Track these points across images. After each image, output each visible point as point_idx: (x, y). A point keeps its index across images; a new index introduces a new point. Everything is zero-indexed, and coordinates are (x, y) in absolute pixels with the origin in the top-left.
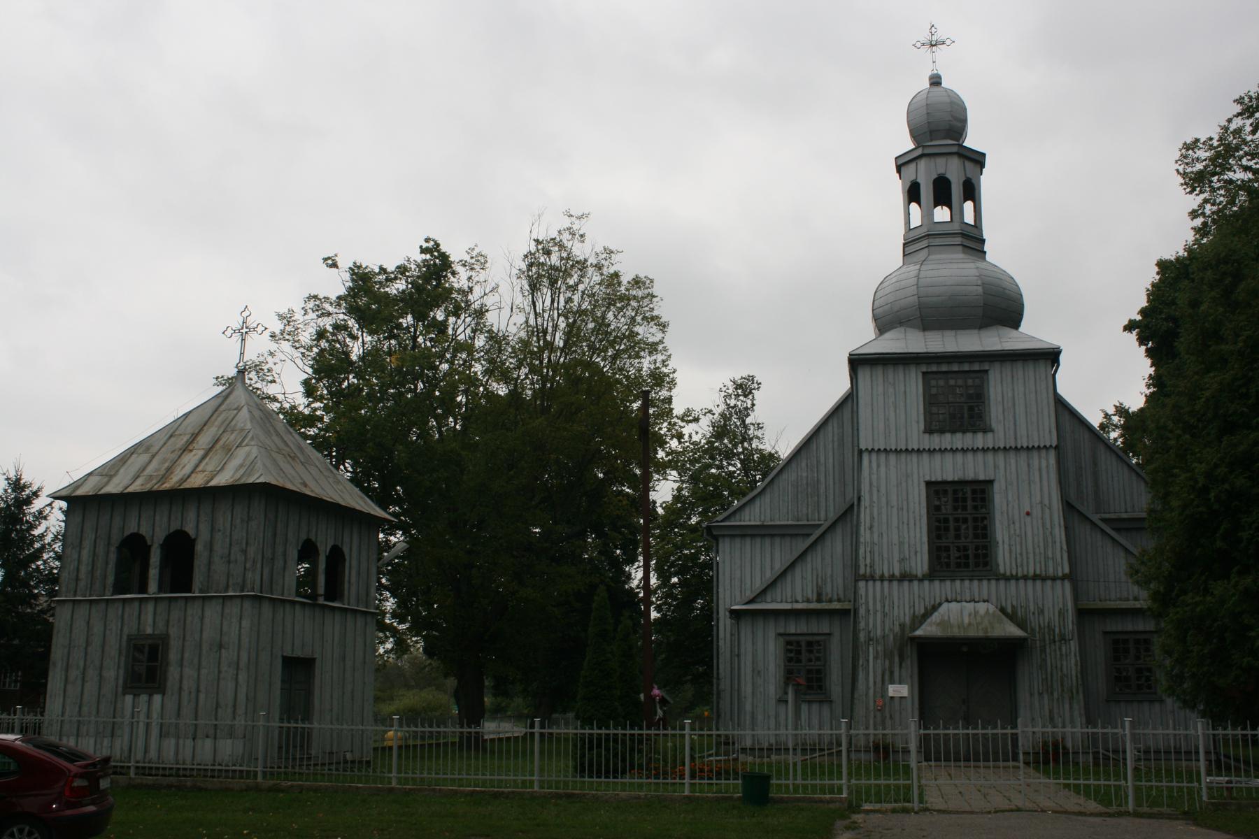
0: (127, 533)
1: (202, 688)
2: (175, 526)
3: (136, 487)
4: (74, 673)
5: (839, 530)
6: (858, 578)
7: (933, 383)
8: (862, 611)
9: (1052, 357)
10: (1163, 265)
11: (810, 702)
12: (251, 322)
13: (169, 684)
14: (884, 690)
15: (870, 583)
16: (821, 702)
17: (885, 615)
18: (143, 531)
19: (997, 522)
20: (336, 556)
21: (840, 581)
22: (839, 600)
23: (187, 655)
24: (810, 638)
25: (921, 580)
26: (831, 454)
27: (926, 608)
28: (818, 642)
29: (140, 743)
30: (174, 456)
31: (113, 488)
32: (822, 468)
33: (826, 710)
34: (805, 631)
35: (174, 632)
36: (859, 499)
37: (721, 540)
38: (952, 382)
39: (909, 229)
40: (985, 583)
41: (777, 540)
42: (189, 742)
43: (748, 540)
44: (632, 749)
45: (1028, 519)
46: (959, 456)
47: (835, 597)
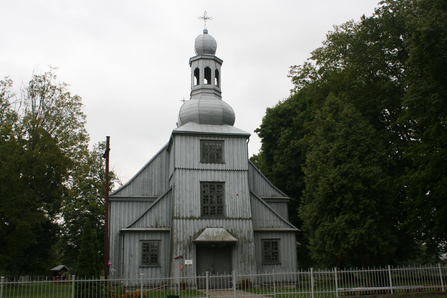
5: (165, 199)
8: (175, 231)
10: (269, 110)
11: (152, 267)
15: (178, 220)
17: (184, 233)
19: (226, 198)
21: (165, 219)
22: (164, 227)
25: (198, 219)
26: (157, 170)
27: (199, 230)
32: (153, 176)
33: (158, 270)
34: (151, 239)
37: (112, 203)
38: (211, 144)
41: (135, 203)
43: (123, 203)
45: (237, 197)
46: (213, 172)
47: (163, 226)
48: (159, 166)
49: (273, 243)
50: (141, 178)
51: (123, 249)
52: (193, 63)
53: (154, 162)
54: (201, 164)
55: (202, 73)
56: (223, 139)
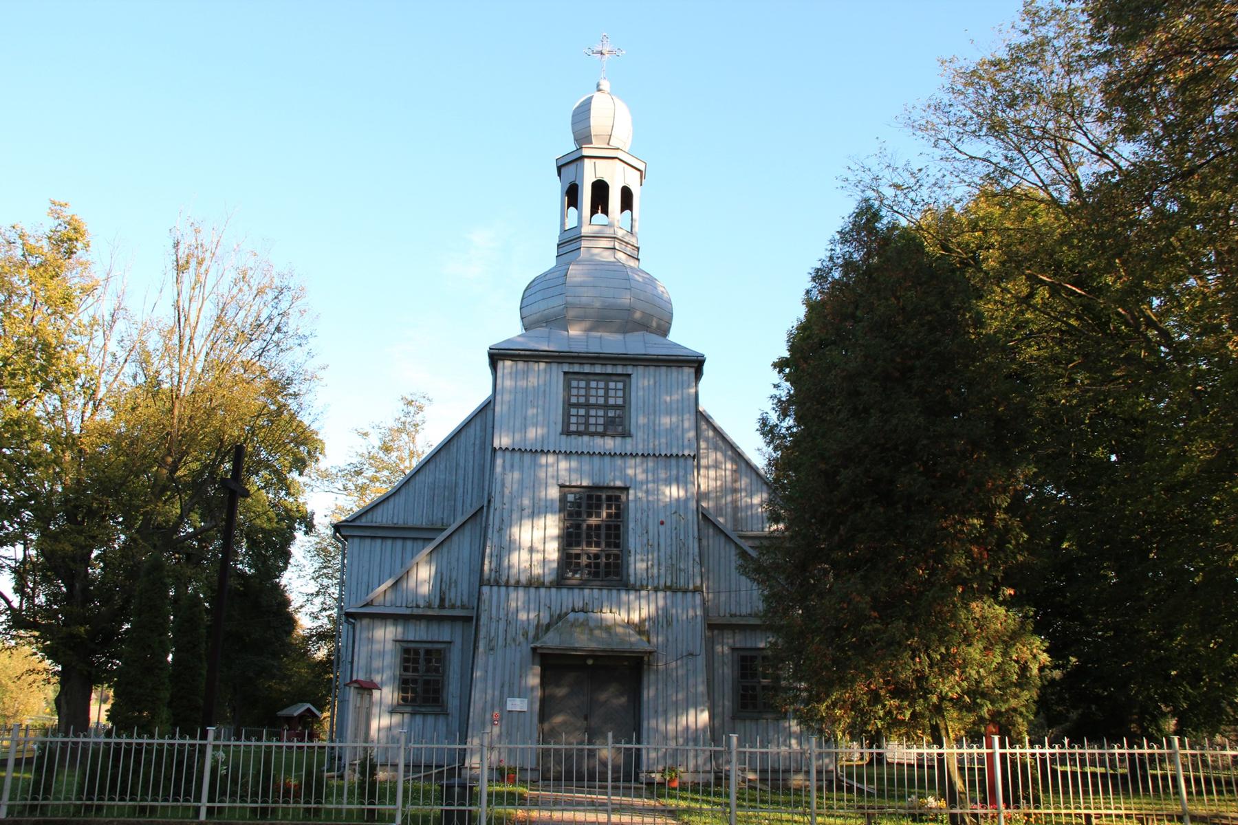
6: (482, 583)
7: (574, 383)
9: (696, 364)
11: (425, 714)
14: (503, 704)
15: (495, 589)
16: (437, 714)
17: (508, 623)
21: (465, 586)
22: (463, 607)
26: (471, 457)
27: (551, 616)
28: (439, 651)
32: (461, 472)
33: (441, 720)
34: (425, 638)
36: (489, 501)
39: (563, 231)
40: (614, 592)
43: (379, 542)
45: (662, 528)
46: (596, 459)
47: (459, 603)
48: (477, 448)
50: (426, 478)
51: (352, 662)
52: (563, 170)
53: (464, 433)
54: (564, 437)
56: (629, 370)
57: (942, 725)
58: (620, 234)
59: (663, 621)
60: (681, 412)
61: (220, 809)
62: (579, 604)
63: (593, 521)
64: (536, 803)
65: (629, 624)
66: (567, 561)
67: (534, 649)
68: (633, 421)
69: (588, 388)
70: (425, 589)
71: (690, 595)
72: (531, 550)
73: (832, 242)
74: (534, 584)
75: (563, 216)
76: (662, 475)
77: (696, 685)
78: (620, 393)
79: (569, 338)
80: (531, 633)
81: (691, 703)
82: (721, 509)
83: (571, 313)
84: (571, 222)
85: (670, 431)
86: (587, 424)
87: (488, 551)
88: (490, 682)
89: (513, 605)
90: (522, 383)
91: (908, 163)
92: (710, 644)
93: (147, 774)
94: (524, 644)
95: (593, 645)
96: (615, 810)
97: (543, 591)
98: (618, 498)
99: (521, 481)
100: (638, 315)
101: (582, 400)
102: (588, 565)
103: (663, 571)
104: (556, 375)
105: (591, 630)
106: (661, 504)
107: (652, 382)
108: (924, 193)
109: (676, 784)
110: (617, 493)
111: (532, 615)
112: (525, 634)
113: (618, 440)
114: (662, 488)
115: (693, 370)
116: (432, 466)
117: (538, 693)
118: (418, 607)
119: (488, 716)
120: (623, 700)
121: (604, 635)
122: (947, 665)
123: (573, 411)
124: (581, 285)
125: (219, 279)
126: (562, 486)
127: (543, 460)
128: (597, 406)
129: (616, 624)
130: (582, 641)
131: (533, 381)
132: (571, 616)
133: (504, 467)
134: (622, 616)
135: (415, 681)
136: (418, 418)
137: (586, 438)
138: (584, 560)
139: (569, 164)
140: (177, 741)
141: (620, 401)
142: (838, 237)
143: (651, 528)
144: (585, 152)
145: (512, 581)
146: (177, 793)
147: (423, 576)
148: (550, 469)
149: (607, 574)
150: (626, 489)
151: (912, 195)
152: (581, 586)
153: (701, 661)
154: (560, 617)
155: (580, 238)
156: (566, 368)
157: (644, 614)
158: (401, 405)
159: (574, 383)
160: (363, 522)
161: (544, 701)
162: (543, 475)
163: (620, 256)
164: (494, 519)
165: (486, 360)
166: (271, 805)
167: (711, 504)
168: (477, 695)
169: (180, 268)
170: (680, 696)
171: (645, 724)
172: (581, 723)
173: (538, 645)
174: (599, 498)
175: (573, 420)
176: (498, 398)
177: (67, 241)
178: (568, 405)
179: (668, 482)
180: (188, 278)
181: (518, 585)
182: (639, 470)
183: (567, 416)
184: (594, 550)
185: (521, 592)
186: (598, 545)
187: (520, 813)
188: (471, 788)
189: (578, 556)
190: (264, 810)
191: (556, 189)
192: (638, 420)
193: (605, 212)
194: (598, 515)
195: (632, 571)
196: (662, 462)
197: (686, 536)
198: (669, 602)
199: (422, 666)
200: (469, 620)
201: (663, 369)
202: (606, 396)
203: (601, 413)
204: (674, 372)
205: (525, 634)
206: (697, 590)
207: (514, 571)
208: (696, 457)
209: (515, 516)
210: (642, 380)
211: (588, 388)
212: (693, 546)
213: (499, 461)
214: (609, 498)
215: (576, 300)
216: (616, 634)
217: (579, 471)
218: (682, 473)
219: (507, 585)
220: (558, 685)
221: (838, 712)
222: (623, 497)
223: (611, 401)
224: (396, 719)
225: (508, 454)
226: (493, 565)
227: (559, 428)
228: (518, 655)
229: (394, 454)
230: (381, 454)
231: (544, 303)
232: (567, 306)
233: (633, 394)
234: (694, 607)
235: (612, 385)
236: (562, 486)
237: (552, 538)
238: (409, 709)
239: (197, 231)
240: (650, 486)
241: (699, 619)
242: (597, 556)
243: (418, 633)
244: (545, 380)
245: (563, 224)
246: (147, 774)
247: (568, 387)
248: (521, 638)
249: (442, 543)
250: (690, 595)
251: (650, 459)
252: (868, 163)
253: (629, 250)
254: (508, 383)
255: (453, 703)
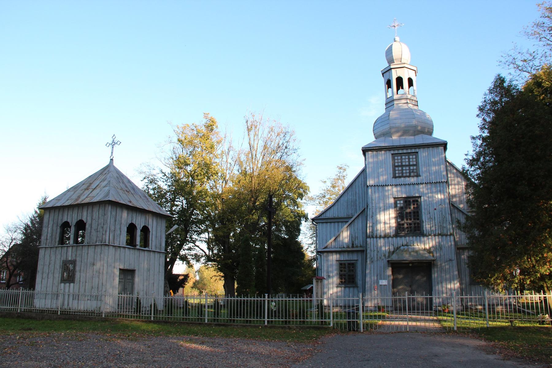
0: (63, 221)
1: (87, 281)
2: (79, 218)
3: (66, 204)
4: (45, 275)
6: (367, 237)
7: (396, 158)
8: (368, 251)
9: (444, 145)
11: (349, 287)
12: (116, 141)
13: (76, 279)
14: (378, 282)
15: (372, 239)
16: (354, 287)
17: (378, 252)
18: (69, 221)
20: (145, 230)
21: (361, 239)
22: (361, 247)
23: (82, 268)
24: (349, 262)
27: (394, 248)
28: (353, 264)
29: (66, 303)
30: (82, 192)
31: (59, 204)
32: (357, 195)
33: (356, 290)
34: (347, 259)
35: (78, 259)
39: (387, 98)
40: (418, 237)
42: (44, 301)
43: (329, 224)
44: (307, 308)
45: (435, 211)
46: (407, 186)
47: (359, 245)
49: (349, 264)
50: (345, 198)
53: (357, 181)
54: (394, 179)
55: (406, 83)
56: (417, 150)
57: (545, 285)
58: (409, 97)
59: (439, 247)
60: (439, 165)
61: (272, 321)
62: (405, 243)
63: (408, 210)
64: (396, 319)
65: (425, 249)
66: (399, 227)
67: (388, 261)
68: (421, 170)
69: (401, 159)
70: (346, 240)
71: (448, 237)
72: (385, 223)
73: (485, 94)
74: (386, 236)
75: (387, 92)
76: (434, 191)
77: (453, 272)
78: (414, 160)
79: (392, 140)
80: (387, 255)
81: (451, 280)
82: (462, 201)
83: (393, 130)
84: (389, 95)
85: (436, 172)
86: (402, 173)
87: (368, 225)
88: (372, 274)
89: (379, 245)
90: (375, 160)
91: (528, 49)
92: (458, 255)
93: (247, 310)
94: (385, 260)
95: (411, 259)
96: (410, 321)
97: (390, 239)
98: (417, 201)
99: (379, 197)
100: (419, 128)
101: (400, 164)
102: (407, 228)
103: (437, 228)
104: (389, 154)
105: (410, 253)
106: (435, 202)
107: (427, 154)
108: (537, 62)
109: (447, 311)
110: (417, 199)
111: (387, 248)
112: (385, 256)
113: (415, 178)
114: (434, 195)
115: (442, 148)
116: (346, 194)
117: (392, 277)
118: (344, 247)
119: (373, 286)
120: (425, 279)
121: (415, 254)
122: (544, 261)
123: (397, 169)
124: (395, 119)
125: (263, 132)
126: (395, 198)
127: (387, 188)
128: (406, 166)
129: (419, 250)
130: (407, 257)
131: (380, 158)
132: (402, 248)
133: (372, 193)
134: (422, 246)
135: (345, 275)
136: (344, 174)
137: (402, 179)
138: (406, 226)
139: (387, 72)
140: (256, 299)
141: (415, 163)
142: (488, 91)
143: (431, 211)
144: (392, 67)
145: (378, 236)
146: (257, 316)
147: (345, 236)
148: (390, 192)
149: (415, 231)
150: (420, 197)
151: (531, 63)
152: (405, 236)
153: (455, 262)
154: (398, 248)
155: (393, 100)
156: (392, 152)
157: (431, 245)
158: (338, 170)
159: (396, 158)
160: (323, 217)
161: (393, 280)
162: (387, 194)
163: (410, 105)
164: (370, 213)
165: (362, 152)
166: (288, 320)
167: (457, 199)
168: (368, 279)
169: (249, 130)
170: (448, 276)
171: (434, 288)
172: (409, 289)
173: (389, 259)
174: (410, 201)
175: (397, 172)
176: (367, 166)
177: (210, 127)
178: (394, 166)
179: (437, 192)
180: (252, 133)
181: (380, 237)
182: (424, 190)
183: (394, 171)
184: (409, 221)
185: (382, 240)
186: (410, 219)
187: (380, 322)
188: (357, 313)
189: (403, 224)
190: (286, 322)
191: (382, 82)
192: (423, 169)
193: (402, 88)
194: (410, 208)
195: (424, 229)
196: (433, 185)
197: (445, 213)
198: (440, 240)
199: (347, 270)
200: (363, 251)
201: (431, 149)
202: (409, 161)
203: (407, 168)
204: (435, 149)
205: (385, 256)
206: (451, 235)
207: (379, 232)
208: (447, 182)
209: (377, 211)
210: (423, 154)
211: (401, 159)
212: (449, 217)
213: (370, 191)
214: (413, 201)
215: (394, 125)
216: (420, 254)
217: (401, 192)
218: (442, 188)
219: (376, 237)
220: (400, 274)
221: (499, 281)
222: (419, 200)
223: (411, 163)
224: (339, 289)
225: (373, 188)
226: (371, 230)
227: (392, 176)
228: (382, 265)
229: (337, 188)
230: (332, 189)
231: (382, 128)
232: (391, 128)
233: (420, 160)
234: (451, 242)
235: (411, 157)
236: (395, 198)
237: (392, 218)
238: (343, 286)
239: (253, 116)
240: (430, 195)
241: (453, 246)
242: (410, 224)
243: (345, 257)
244: (385, 157)
245: (386, 96)
246: (247, 310)
247: (394, 159)
248: (383, 257)
249: (351, 223)
250: (448, 237)
251: (429, 185)
252: (510, 53)
253: (414, 102)
254: (371, 160)
255: (360, 283)
